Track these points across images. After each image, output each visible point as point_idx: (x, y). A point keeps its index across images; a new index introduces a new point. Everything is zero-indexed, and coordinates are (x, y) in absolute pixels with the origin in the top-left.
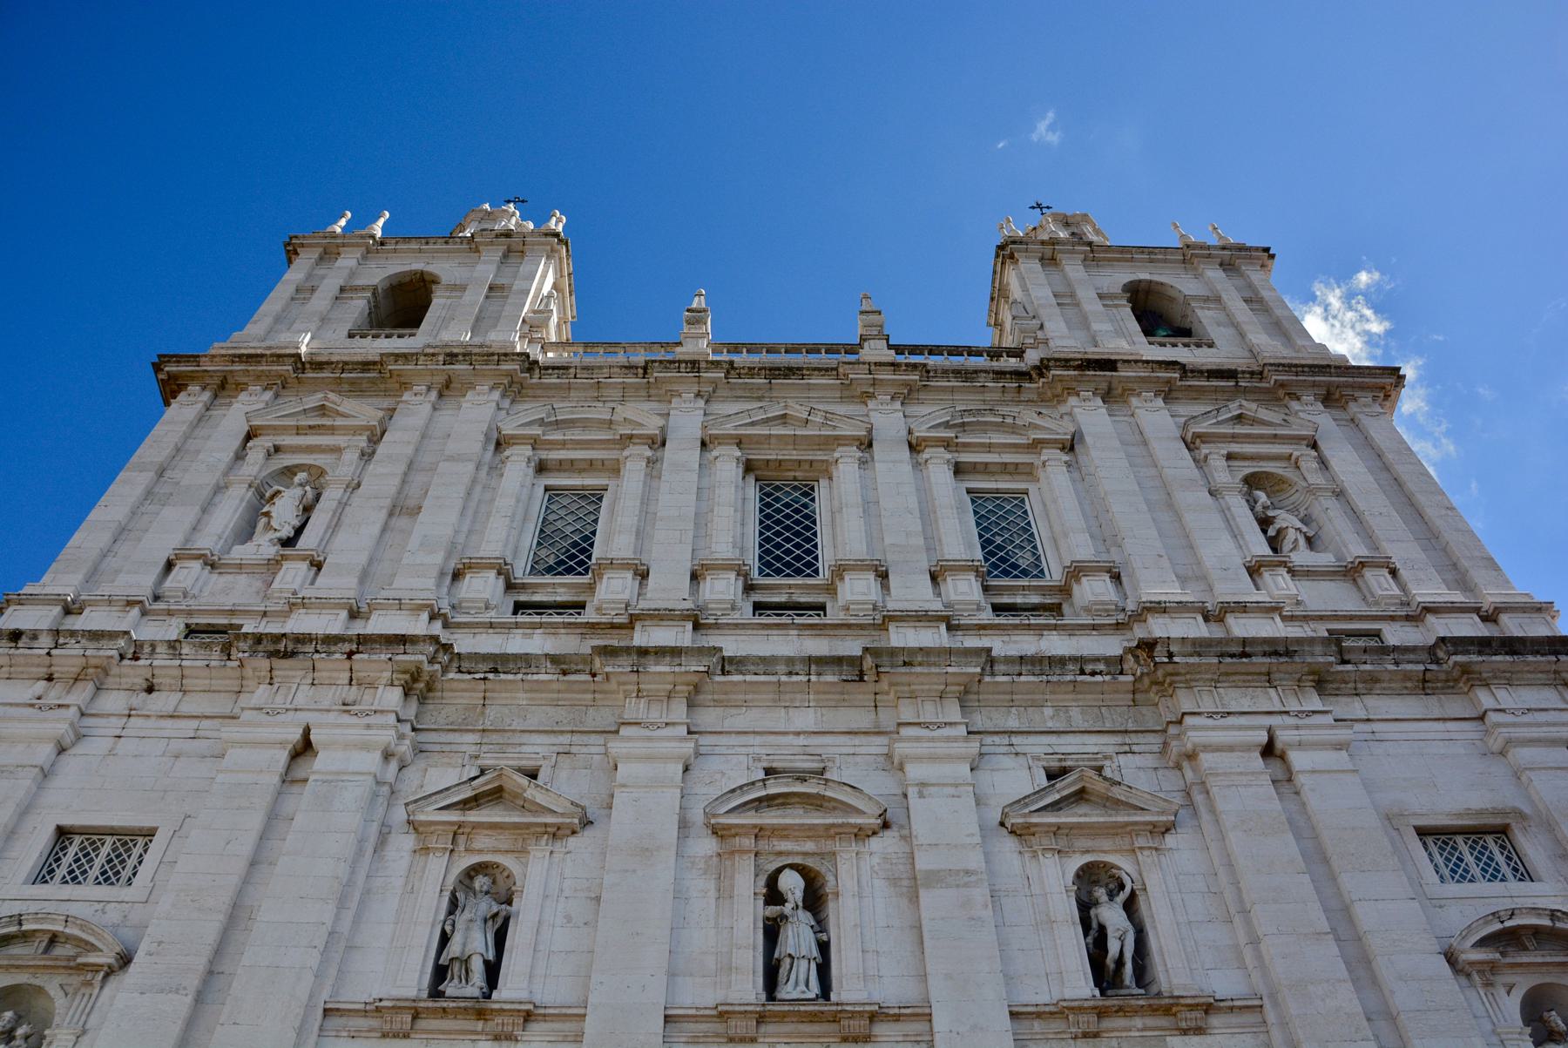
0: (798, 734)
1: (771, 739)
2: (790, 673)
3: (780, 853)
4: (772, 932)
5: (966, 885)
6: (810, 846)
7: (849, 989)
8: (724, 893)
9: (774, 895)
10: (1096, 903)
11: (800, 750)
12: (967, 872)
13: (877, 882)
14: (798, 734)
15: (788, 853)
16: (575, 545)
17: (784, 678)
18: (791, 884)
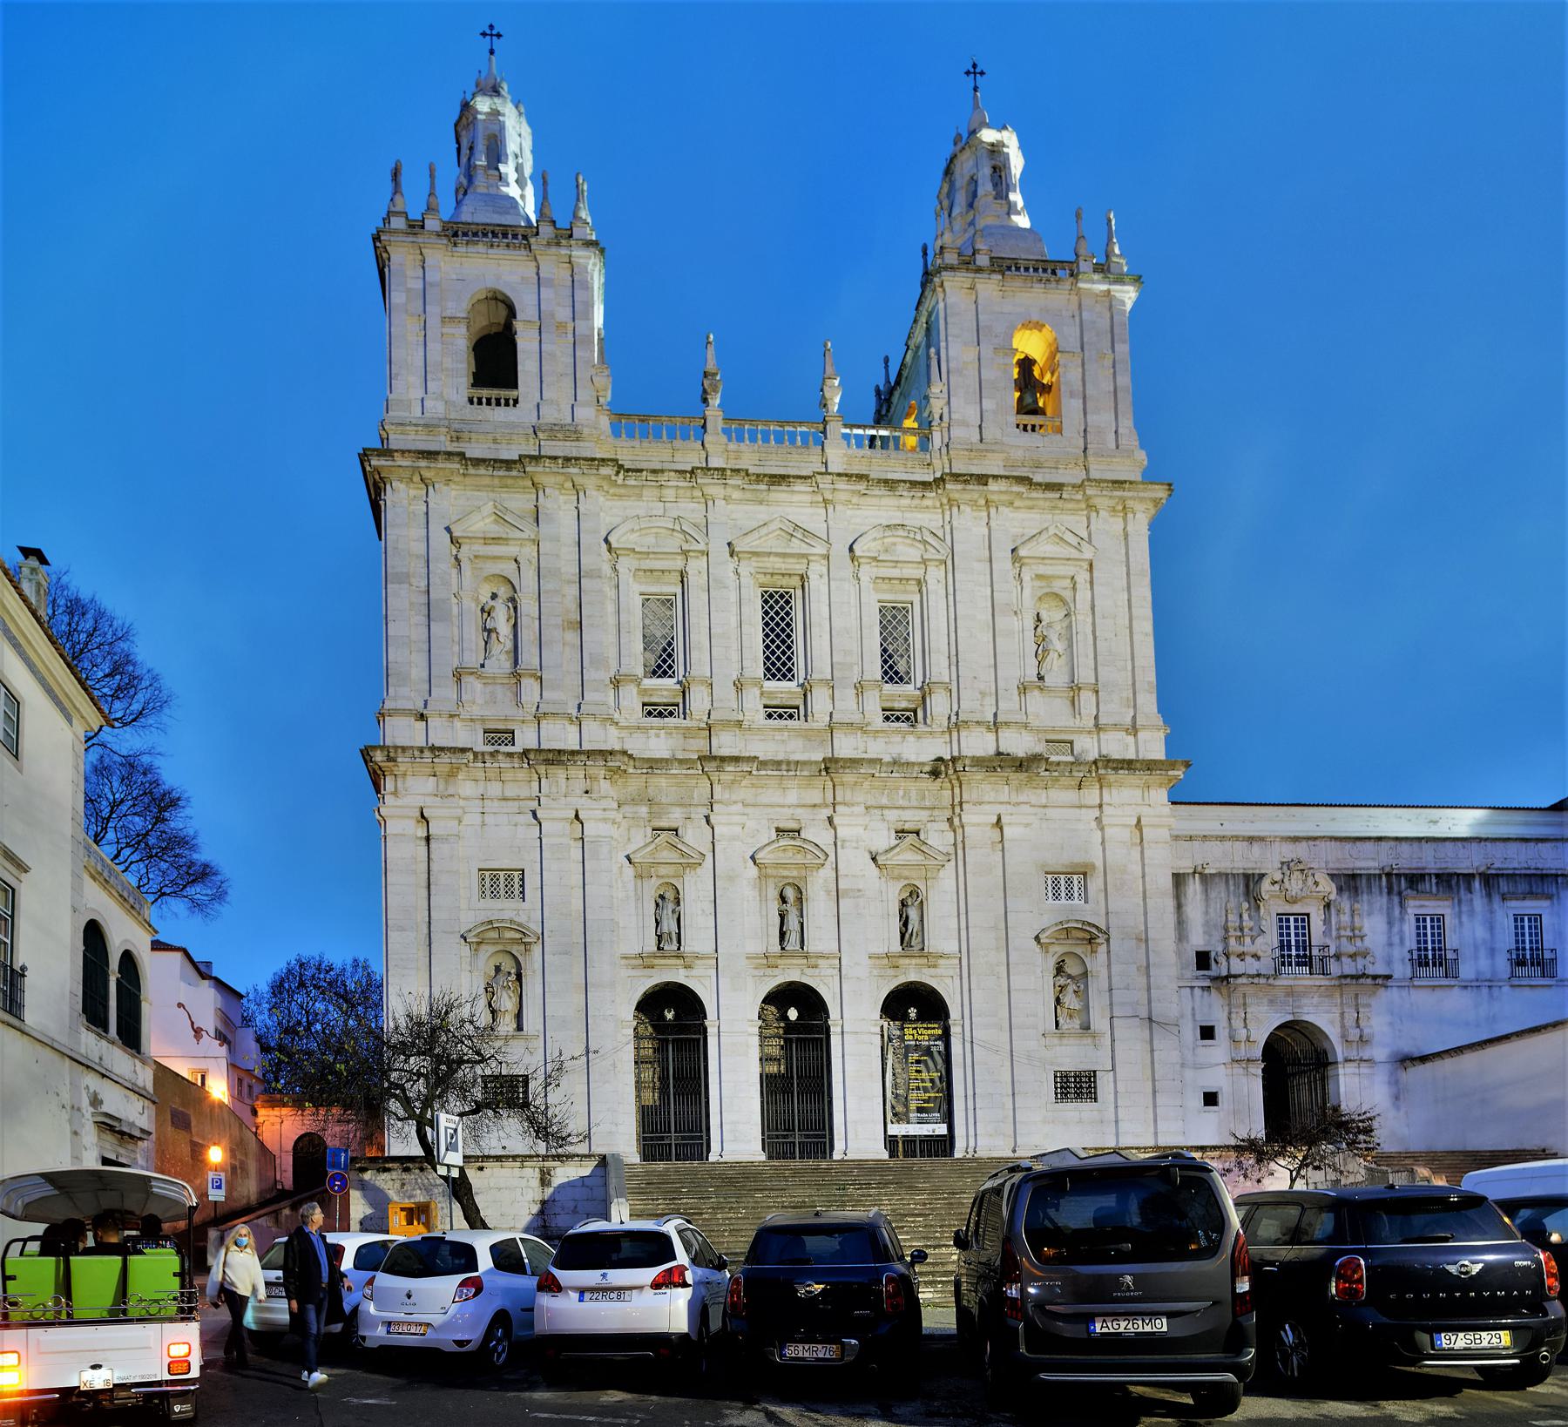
0: (789, 807)
1: (778, 809)
2: (788, 771)
3: (783, 877)
4: (782, 917)
5: (858, 897)
6: (795, 873)
7: (812, 946)
8: (763, 898)
9: (783, 900)
10: (907, 906)
11: (790, 817)
12: (859, 891)
13: (822, 893)
14: (789, 807)
15: (787, 877)
16: (665, 650)
17: (785, 773)
18: (790, 893)
